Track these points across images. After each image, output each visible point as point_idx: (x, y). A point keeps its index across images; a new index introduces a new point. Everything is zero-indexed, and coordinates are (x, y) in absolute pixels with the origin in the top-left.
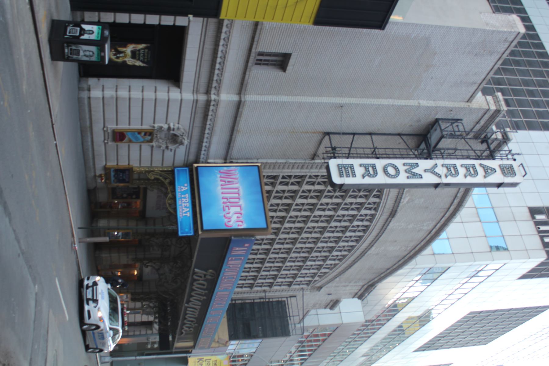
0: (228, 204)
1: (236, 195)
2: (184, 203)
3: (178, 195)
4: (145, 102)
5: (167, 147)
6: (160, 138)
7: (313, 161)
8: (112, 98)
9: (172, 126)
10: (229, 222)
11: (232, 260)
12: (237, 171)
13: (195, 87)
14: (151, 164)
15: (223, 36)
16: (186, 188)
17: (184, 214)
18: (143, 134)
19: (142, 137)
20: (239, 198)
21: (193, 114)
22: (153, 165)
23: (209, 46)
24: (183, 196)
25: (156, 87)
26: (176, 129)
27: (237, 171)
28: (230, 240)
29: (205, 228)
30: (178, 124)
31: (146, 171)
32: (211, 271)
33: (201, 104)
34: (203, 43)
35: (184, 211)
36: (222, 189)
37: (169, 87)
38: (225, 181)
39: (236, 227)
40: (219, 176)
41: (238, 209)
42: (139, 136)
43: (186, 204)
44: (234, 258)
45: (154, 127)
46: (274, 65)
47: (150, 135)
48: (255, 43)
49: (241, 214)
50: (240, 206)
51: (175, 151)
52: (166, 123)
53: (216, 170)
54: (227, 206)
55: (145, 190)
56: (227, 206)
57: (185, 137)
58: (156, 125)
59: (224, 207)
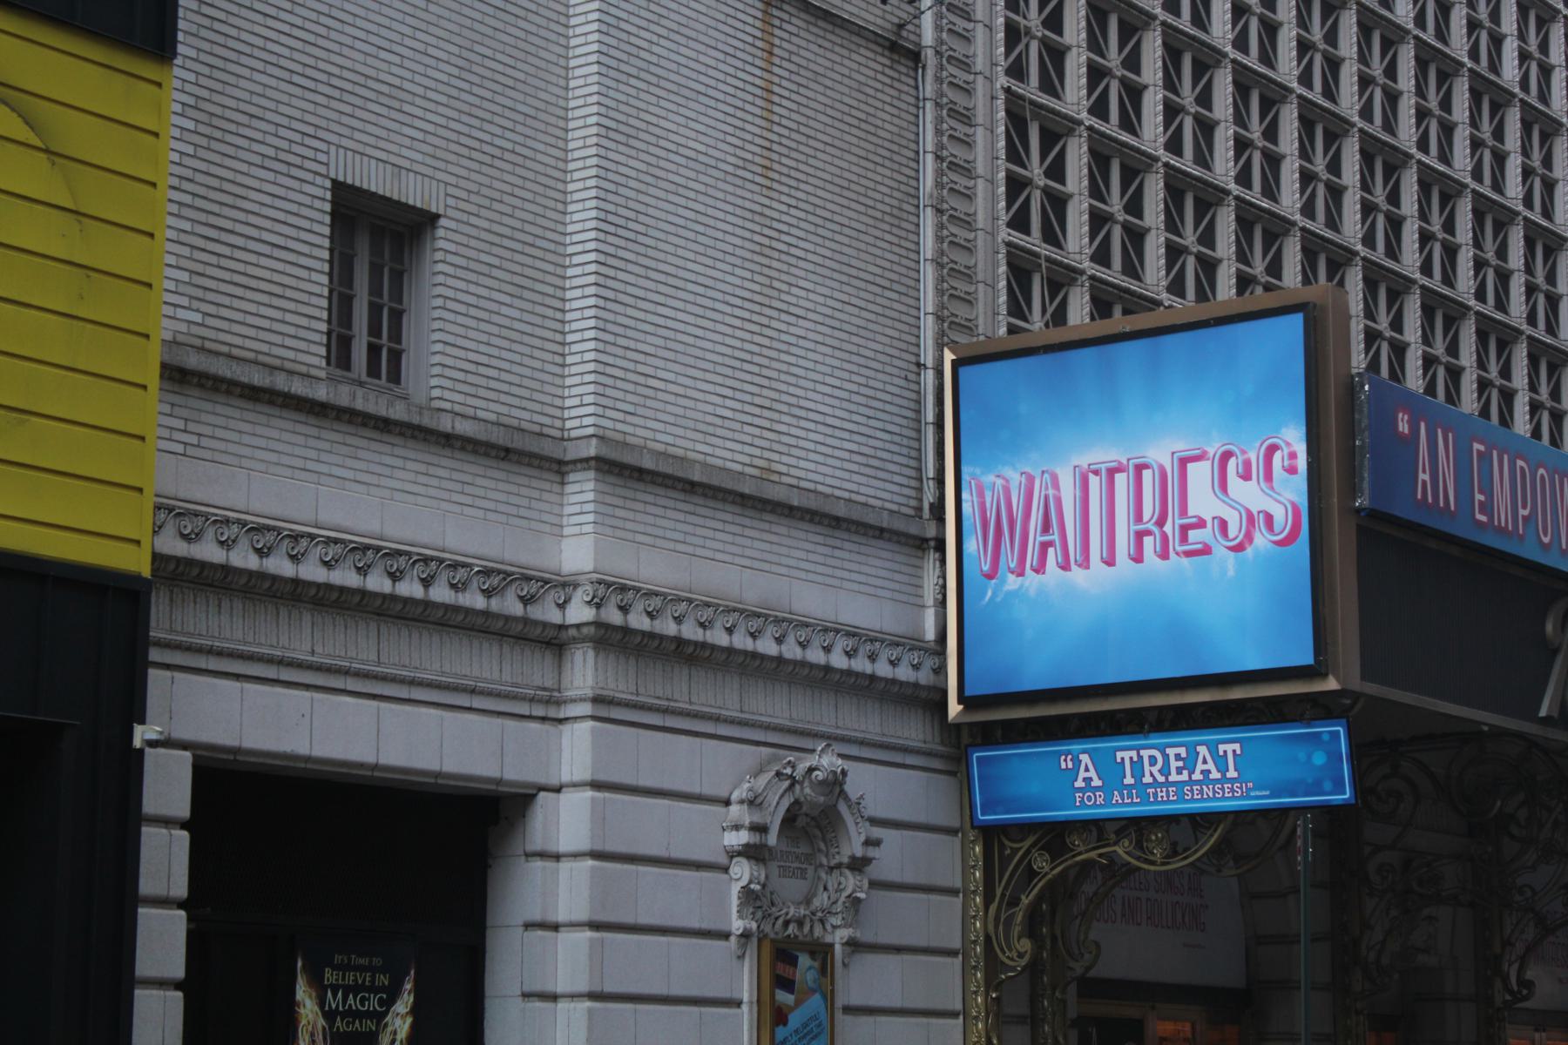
0: (1168, 528)
1: (1120, 479)
2: (1165, 771)
3: (1124, 806)
4: (609, 988)
5: (858, 865)
6: (808, 901)
7: (929, 56)
9: (741, 838)
10: (1269, 519)
11: (1486, 508)
12: (991, 482)
13: (523, 709)
14: (952, 953)
15: (243, 558)
16: (1085, 758)
17: (1232, 774)
18: (784, 997)
19: (798, 1003)
20: (1140, 468)
21: (671, 722)
22: (956, 944)
23: (302, 637)
24: (1129, 780)
25: (529, 926)
27: (989, 479)
28: (1373, 514)
29: (1303, 655)
30: (727, 803)
31: (991, 982)
32: (1549, 628)
33: (621, 680)
34: (282, 670)
35: (1215, 775)
36: (1085, 563)
37: (529, 855)
38: (1045, 546)
39: (1300, 481)
40: (1012, 582)
41: (1200, 474)
42: (795, 1020)
43: (1174, 764)
44: (1479, 497)
45: (745, 935)
46: (398, 278)
47: (793, 961)
48: (281, 382)
49: (1227, 456)
50: (1184, 462)
51: (874, 821)
52: (726, 870)
53: (984, 595)
54: (1184, 539)
55: (1092, 988)
56: (1184, 539)
57: (802, 767)
58: (737, 925)
59: (1189, 554)
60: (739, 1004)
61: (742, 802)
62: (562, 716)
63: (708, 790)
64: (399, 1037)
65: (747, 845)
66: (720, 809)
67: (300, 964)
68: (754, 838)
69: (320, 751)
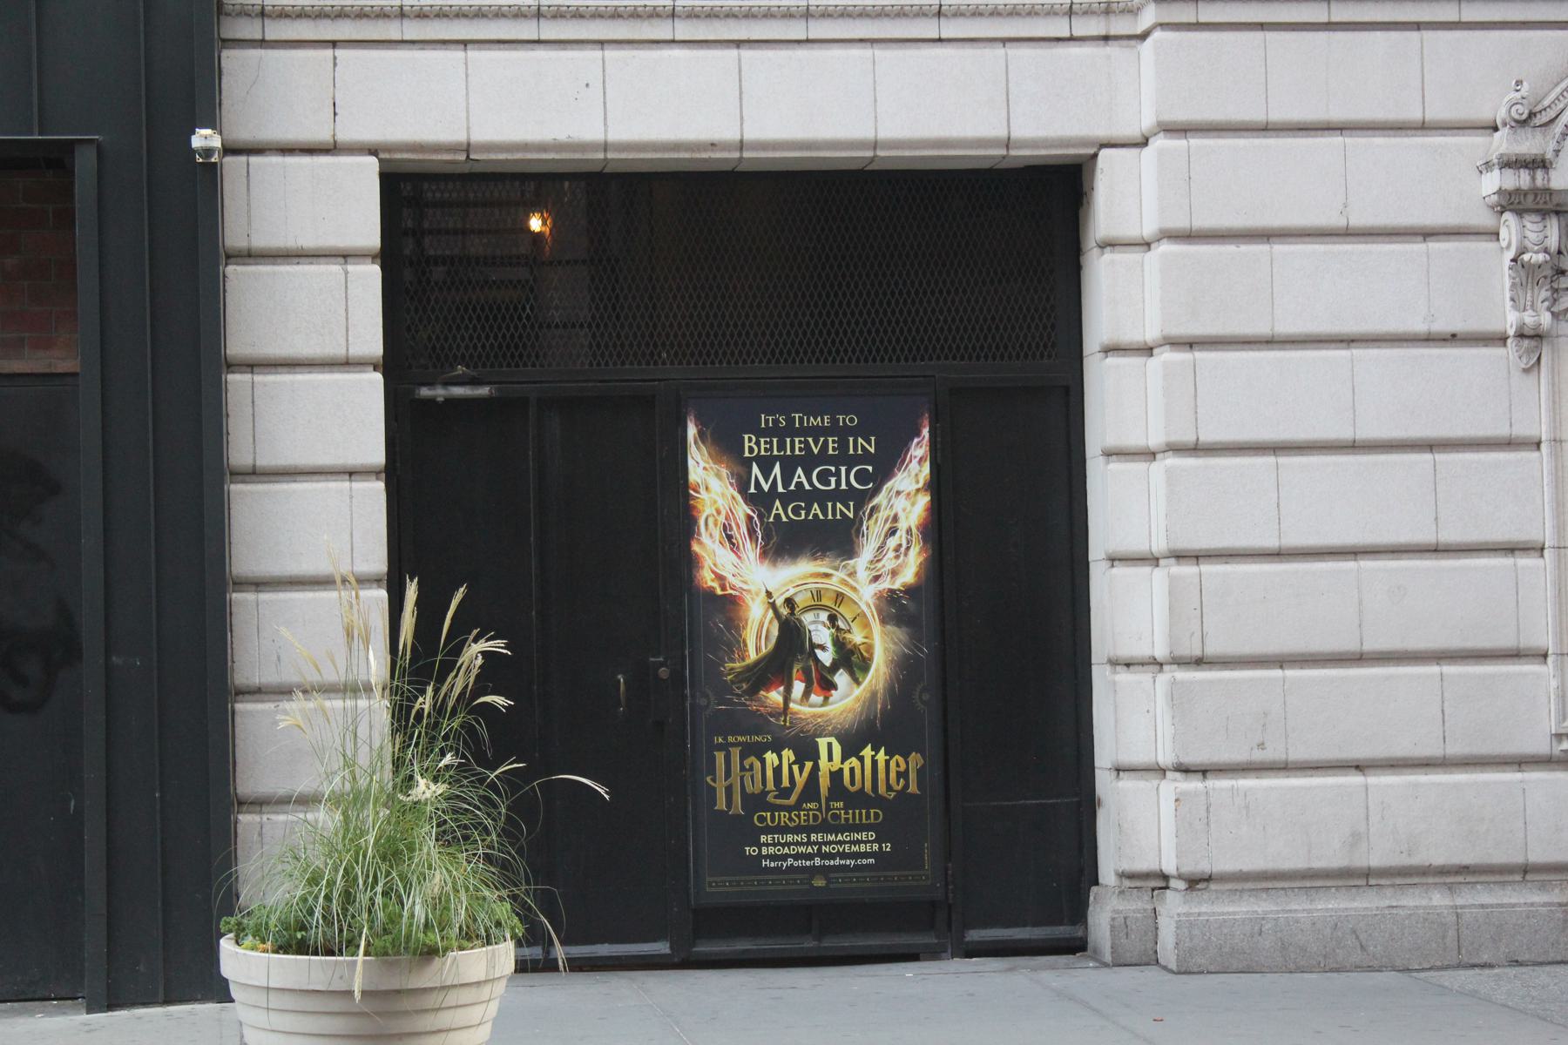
4: (1208, 436)
8: (1178, 699)
9: (1492, 182)
26: (1529, 144)
30: (1496, 129)
52: (1496, 235)
58: (1510, 320)
60: (1538, 445)
61: (1505, 124)
62: (1139, 31)
63: (1437, 111)
64: (902, 525)
65: (1500, 192)
66: (1477, 140)
67: (692, 431)
68: (1523, 179)
69: (622, 132)
